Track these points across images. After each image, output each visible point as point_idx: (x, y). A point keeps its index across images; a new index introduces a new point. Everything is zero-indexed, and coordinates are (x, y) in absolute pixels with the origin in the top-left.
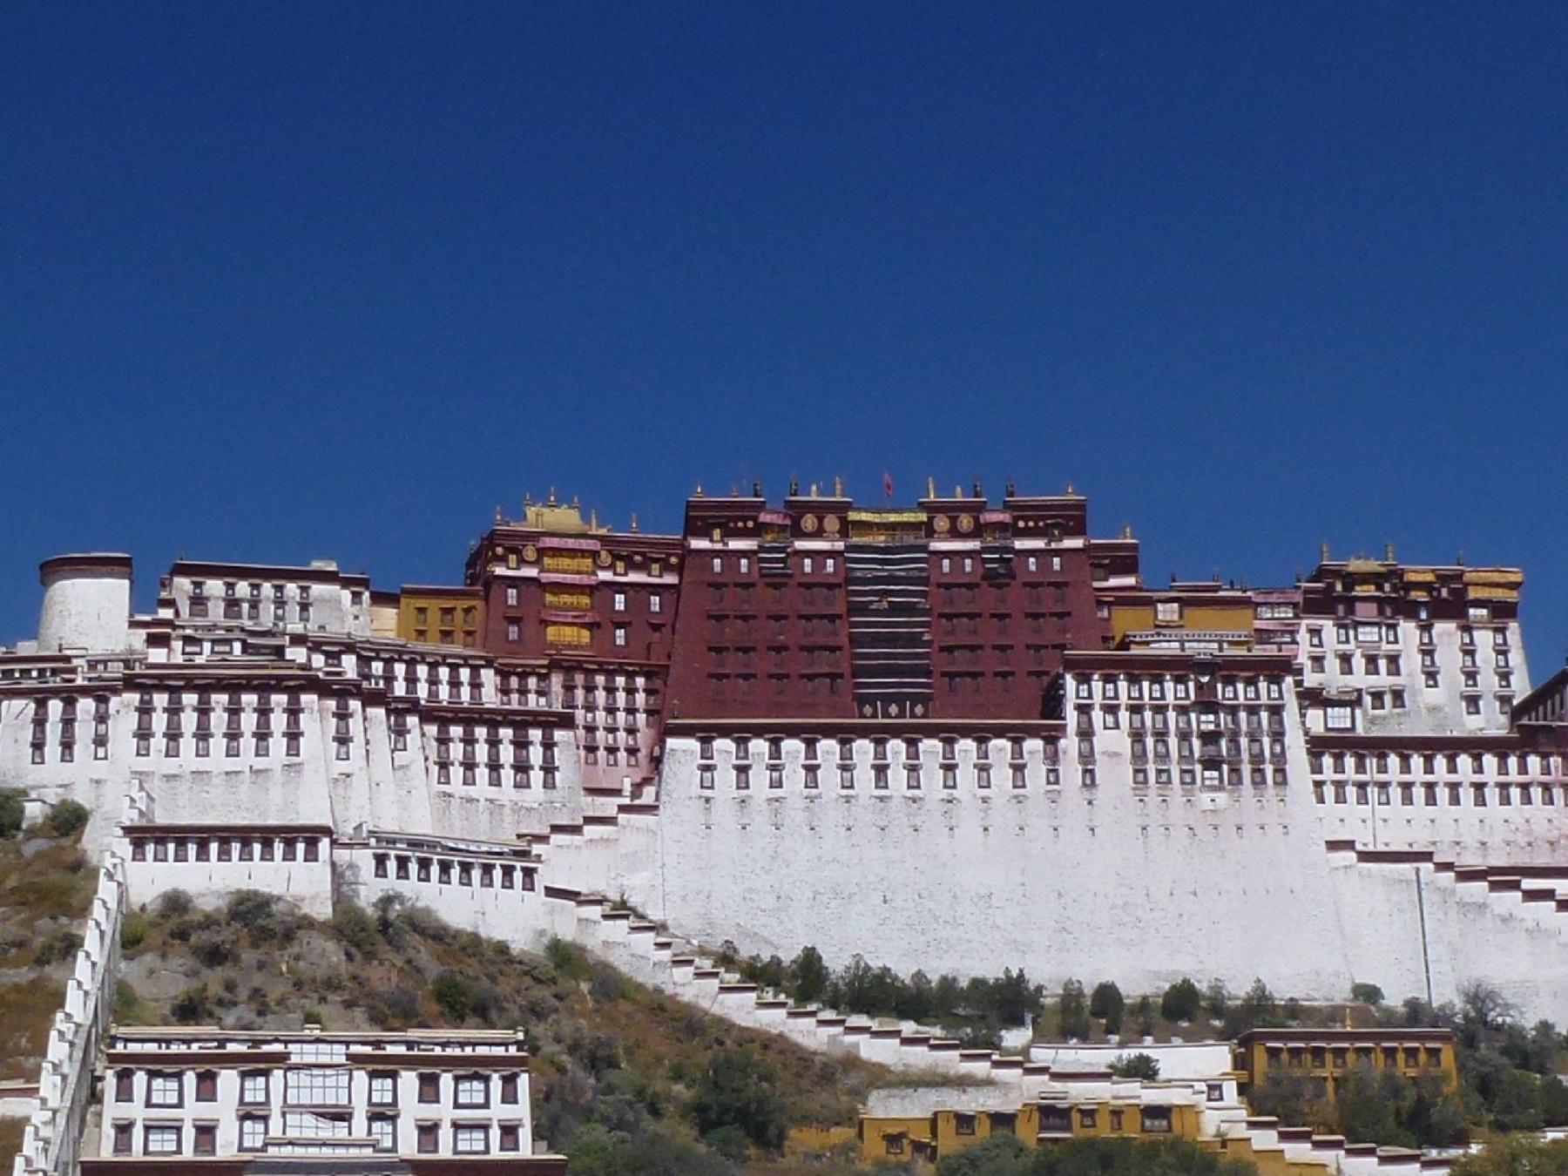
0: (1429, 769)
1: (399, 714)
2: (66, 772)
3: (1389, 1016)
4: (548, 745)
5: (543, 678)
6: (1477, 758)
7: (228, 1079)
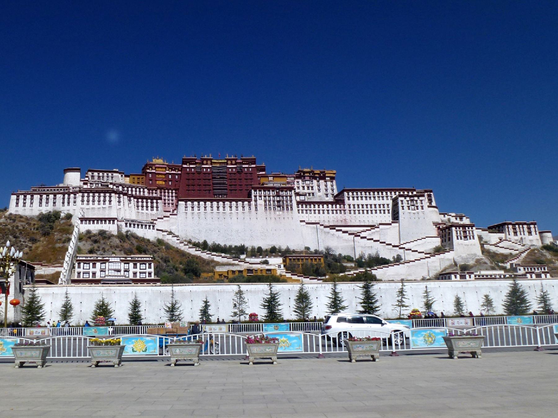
0: (319, 207)
1: (130, 197)
2: (68, 208)
3: (311, 253)
4: (157, 203)
5: (156, 190)
6: (328, 205)
7: (98, 264)
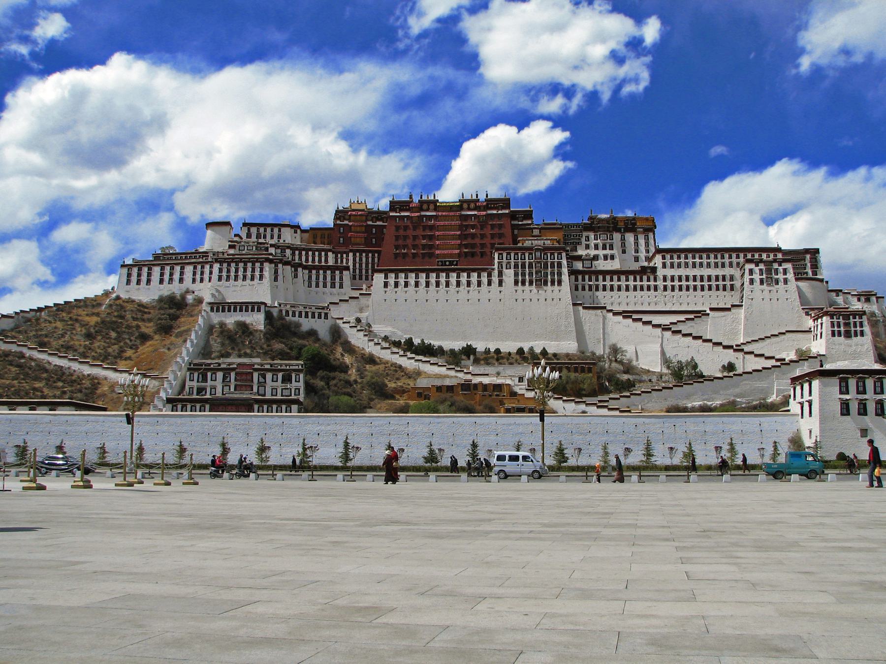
3: (588, 358)
